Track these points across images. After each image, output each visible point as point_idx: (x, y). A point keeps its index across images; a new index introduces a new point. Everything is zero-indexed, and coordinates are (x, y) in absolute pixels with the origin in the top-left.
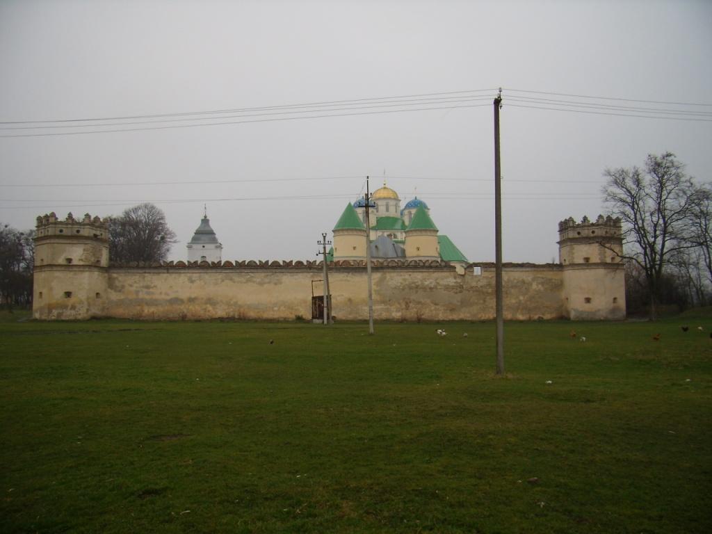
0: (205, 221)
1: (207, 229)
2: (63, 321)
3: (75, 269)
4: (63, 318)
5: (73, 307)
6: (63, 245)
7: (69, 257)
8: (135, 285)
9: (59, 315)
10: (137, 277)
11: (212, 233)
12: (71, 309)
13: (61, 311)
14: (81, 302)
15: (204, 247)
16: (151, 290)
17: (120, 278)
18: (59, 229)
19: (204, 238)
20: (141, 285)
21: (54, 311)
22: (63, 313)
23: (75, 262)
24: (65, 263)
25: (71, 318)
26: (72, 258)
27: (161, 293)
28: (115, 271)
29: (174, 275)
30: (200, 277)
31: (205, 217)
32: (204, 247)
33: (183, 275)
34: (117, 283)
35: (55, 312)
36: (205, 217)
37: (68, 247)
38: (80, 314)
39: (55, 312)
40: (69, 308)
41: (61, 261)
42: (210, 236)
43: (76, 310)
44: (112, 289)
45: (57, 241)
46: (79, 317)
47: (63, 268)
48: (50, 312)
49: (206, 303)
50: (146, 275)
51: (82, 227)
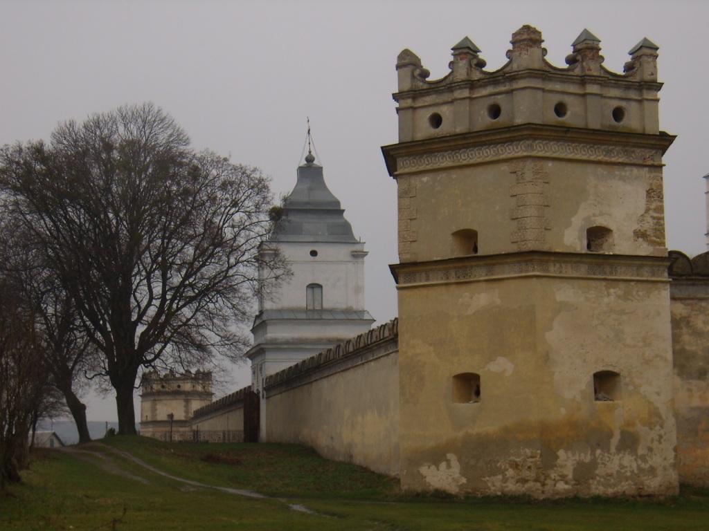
1: (318, 196)
2: (598, 500)
3: (623, 273)
4: (597, 488)
5: (629, 442)
6: (578, 168)
7: (600, 221)
9: (584, 472)
11: (334, 210)
12: (620, 449)
13: (587, 458)
14: (654, 418)
15: (314, 253)
19: (310, 224)
21: (561, 453)
22: (594, 464)
24: (580, 246)
25: (626, 487)
26: (612, 225)
31: (310, 159)
32: (314, 253)
35: (567, 461)
36: (310, 159)
37: (592, 178)
38: (652, 471)
39: (567, 461)
41: (573, 240)
42: (330, 220)
43: (641, 451)
45: (555, 149)
46: (653, 484)
47: (583, 270)
48: (549, 459)
51: (633, 95)
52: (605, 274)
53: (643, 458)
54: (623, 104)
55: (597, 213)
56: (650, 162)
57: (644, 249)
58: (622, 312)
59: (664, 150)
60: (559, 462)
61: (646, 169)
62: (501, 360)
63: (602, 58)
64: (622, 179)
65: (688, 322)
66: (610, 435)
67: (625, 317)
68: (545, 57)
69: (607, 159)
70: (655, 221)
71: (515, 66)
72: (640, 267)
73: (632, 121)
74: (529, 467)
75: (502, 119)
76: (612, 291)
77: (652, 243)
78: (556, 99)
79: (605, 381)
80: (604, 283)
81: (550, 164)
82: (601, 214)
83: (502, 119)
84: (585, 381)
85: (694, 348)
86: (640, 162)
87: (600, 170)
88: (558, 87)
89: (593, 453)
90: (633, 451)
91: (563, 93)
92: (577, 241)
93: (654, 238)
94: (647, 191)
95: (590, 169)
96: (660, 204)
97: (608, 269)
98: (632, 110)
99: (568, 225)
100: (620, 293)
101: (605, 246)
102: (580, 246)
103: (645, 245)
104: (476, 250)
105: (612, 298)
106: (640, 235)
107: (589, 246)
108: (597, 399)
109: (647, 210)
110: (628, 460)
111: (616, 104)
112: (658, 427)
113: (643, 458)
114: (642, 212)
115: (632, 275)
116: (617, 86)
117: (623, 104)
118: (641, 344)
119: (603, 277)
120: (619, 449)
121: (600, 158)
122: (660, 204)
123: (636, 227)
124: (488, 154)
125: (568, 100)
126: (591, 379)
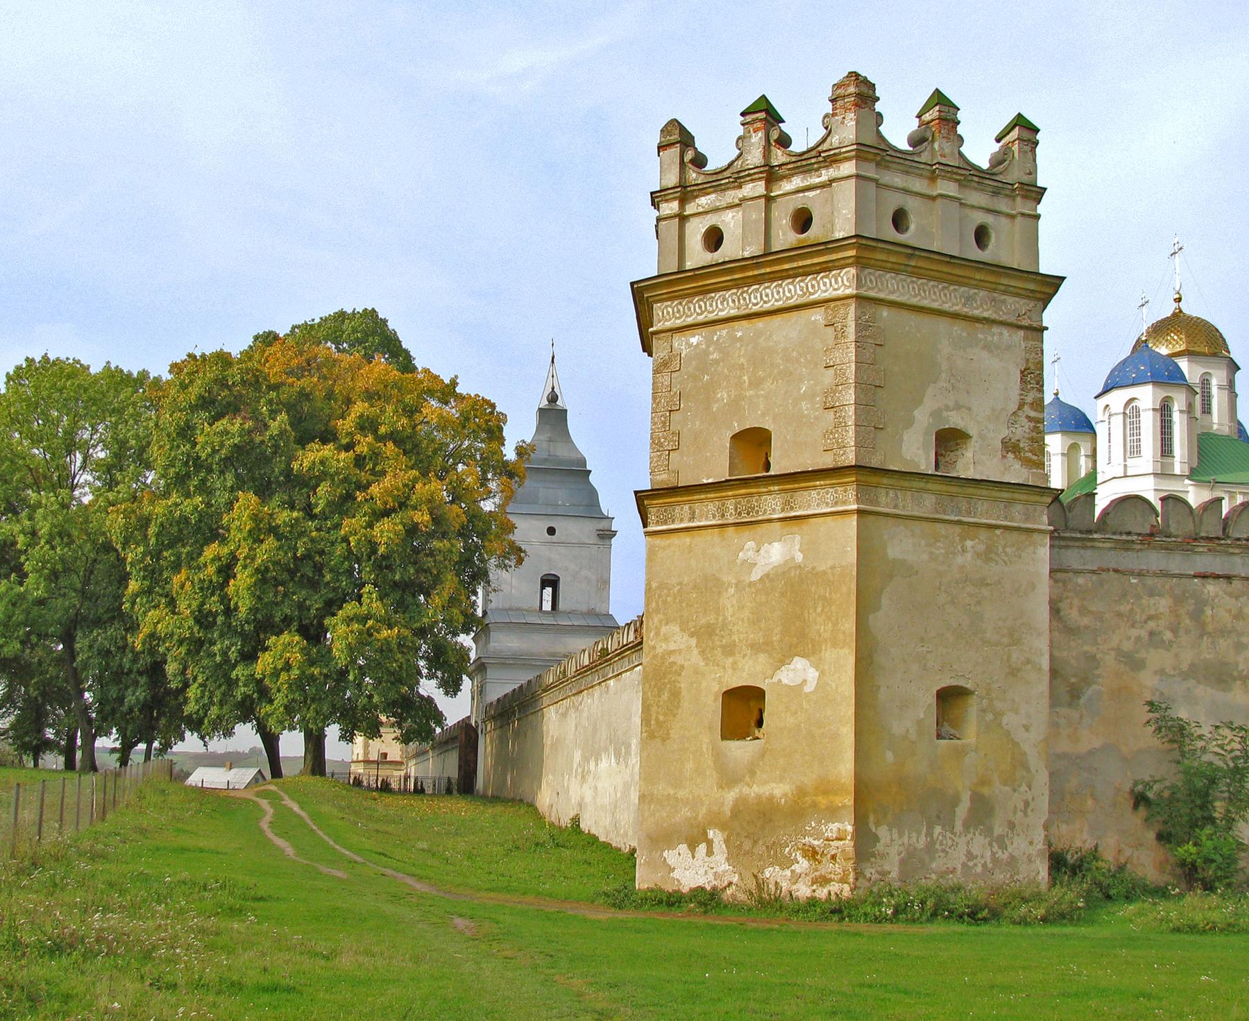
7: (955, 420)
8: (1155, 658)
20: (1187, 657)
24: (924, 461)
40: (962, 810)
47: (927, 504)
50: (1211, 588)
52: (960, 513)
53: (1001, 842)
54: (989, 219)
55: (951, 404)
56: (1026, 322)
57: (1016, 473)
58: (982, 583)
59: (1046, 300)
60: (880, 847)
61: (1021, 333)
62: (799, 663)
63: (961, 139)
64: (987, 347)
66: (955, 801)
67: (985, 592)
68: (880, 128)
70: (1032, 424)
71: (835, 140)
72: (1010, 503)
73: (1001, 250)
74: (833, 857)
75: (815, 233)
76: (969, 543)
77: (1028, 463)
78: (894, 201)
80: (958, 529)
81: (885, 312)
82: (958, 407)
83: (815, 233)
85: (1065, 654)
86: (1013, 319)
87: (958, 328)
88: (898, 180)
89: (929, 833)
91: (906, 191)
92: (921, 452)
93: (1029, 454)
94: (1022, 372)
95: (942, 324)
96: (1039, 395)
97: (964, 505)
98: (1001, 232)
99: (909, 422)
100: (981, 548)
101: (960, 465)
102: (924, 461)
103: (1017, 465)
104: (767, 466)
105: (969, 556)
106: (1010, 447)
107: (937, 467)
108: (939, 737)
109: (1021, 406)
110: (979, 843)
111: (980, 218)
112: (1024, 788)
113: (1001, 842)
114: (1013, 407)
115: (998, 518)
116: (981, 187)
117: (989, 219)
118: (1005, 640)
119: (957, 518)
120: (967, 825)
121: (956, 308)
122: (1039, 395)
123: (1005, 433)
124: (791, 291)
125: (911, 204)
126: (932, 700)
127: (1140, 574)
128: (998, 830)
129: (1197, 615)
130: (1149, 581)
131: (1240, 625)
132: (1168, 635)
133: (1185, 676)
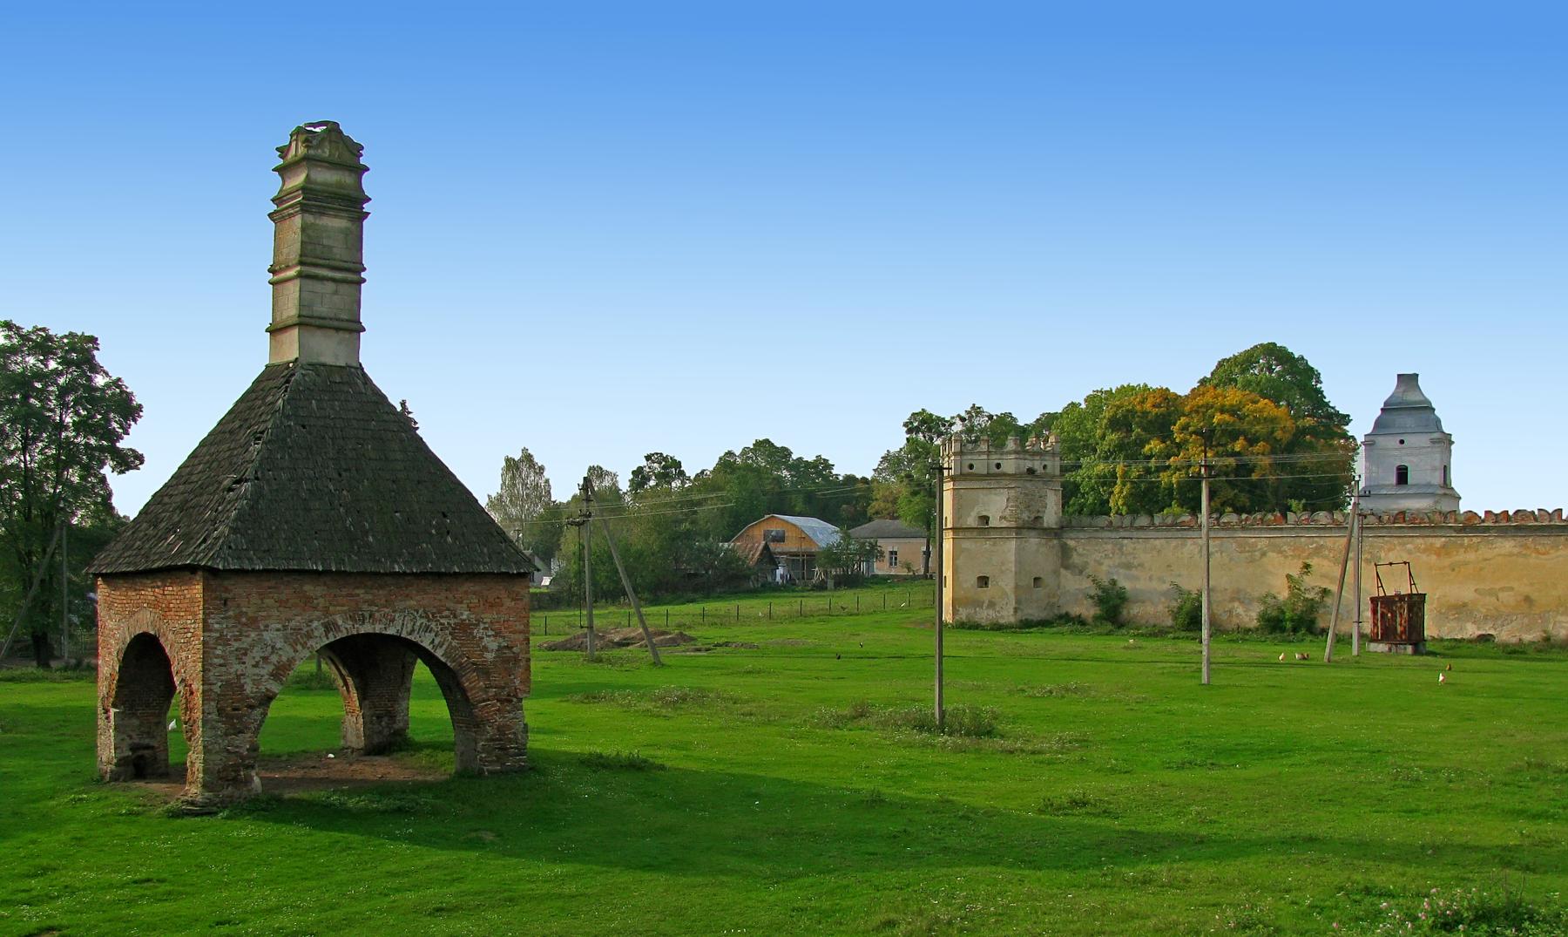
0: (1408, 381)
1: (1412, 397)
5: (992, 605)
6: (975, 492)
7: (984, 513)
8: (1107, 562)
10: (1109, 547)
12: (988, 607)
16: (1134, 572)
17: (1080, 550)
18: (968, 463)
19: (1408, 421)
20: (1117, 561)
23: (993, 523)
27: (1151, 578)
28: (1072, 535)
29: (1174, 543)
30: (1222, 545)
33: (1189, 542)
34: (1076, 559)
40: (985, 605)
44: (1067, 568)
46: (1002, 621)
47: (975, 534)
49: (1232, 600)
50: (1126, 541)
54: (999, 461)
64: (995, 494)
65: (1076, 550)
69: (988, 487)
79: (983, 581)
81: (962, 491)
82: (985, 510)
84: (974, 580)
87: (985, 491)
90: (994, 609)
95: (980, 491)
99: (969, 515)
123: (1001, 514)
127: (1102, 539)
128: (998, 609)
129: (1121, 549)
130: (1105, 540)
131: (1135, 552)
132: (1111, 555)
133: (1116, 567)
